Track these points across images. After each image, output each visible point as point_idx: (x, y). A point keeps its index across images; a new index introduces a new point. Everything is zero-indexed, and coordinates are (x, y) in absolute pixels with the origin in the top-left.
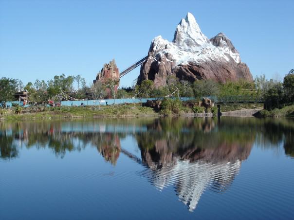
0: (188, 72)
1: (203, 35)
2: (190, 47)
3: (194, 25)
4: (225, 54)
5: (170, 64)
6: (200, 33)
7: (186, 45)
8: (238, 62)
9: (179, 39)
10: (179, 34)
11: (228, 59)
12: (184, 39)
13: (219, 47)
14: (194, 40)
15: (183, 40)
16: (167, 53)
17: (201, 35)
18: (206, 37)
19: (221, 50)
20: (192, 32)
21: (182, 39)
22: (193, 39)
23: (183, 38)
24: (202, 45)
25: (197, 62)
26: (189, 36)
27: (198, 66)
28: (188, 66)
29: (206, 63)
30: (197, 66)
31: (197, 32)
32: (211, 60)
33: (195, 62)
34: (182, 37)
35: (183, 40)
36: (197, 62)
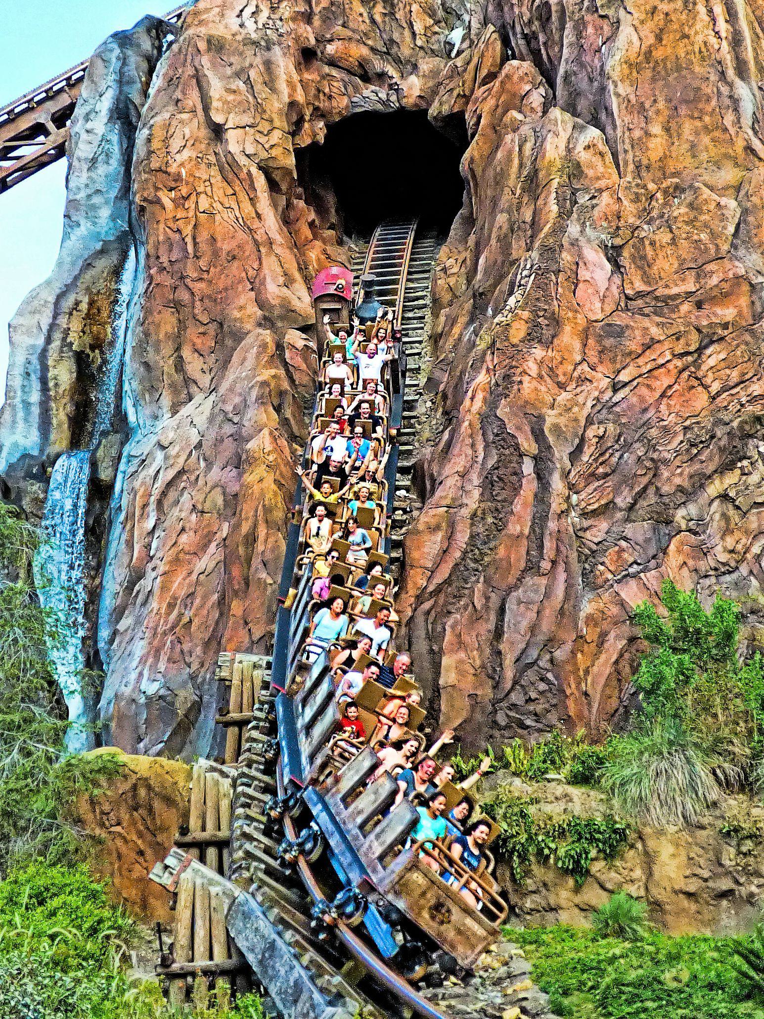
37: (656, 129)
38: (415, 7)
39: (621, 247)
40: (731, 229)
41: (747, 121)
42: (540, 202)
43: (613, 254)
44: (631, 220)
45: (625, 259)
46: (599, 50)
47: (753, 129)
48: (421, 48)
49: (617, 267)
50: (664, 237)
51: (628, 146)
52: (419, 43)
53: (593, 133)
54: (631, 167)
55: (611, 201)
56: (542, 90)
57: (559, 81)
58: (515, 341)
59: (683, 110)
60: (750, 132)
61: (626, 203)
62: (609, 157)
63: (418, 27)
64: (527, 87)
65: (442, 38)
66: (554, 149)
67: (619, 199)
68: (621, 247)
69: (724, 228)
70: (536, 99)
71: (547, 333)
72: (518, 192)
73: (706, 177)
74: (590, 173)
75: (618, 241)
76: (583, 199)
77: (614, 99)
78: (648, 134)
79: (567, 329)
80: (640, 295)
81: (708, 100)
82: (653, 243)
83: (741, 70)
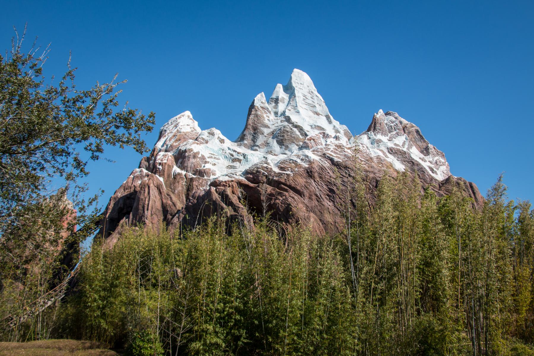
0: (403, 270)
1: (336, 123)
3: (309, 96)
4: (391, 151)
5: (183, 183)
6: (328, 117)
7: (274, 144)
8: (440, 177)
9: (255, 129)
10: (257, 116)
11: (400, 166)
12: (273, 128)
13: (371, 133)
14: (300, 129)
15: (266, 131)
17: (330, 122)
18: (345, 127)
19: (379, 141)
20: (298, 112)
22: (296, 127)
23: (267, 127)
25: (277, 170)
26: (288, 119)
27: (276, 184)
28: (240, 184)
29: (309, 173)
30: (270, 182)
31: (318, 114)
32: (332, 160)
33: (270, 170)
34: (266, 122)
35: (266, 131)
36: (277, 170)
83: (148, 210)
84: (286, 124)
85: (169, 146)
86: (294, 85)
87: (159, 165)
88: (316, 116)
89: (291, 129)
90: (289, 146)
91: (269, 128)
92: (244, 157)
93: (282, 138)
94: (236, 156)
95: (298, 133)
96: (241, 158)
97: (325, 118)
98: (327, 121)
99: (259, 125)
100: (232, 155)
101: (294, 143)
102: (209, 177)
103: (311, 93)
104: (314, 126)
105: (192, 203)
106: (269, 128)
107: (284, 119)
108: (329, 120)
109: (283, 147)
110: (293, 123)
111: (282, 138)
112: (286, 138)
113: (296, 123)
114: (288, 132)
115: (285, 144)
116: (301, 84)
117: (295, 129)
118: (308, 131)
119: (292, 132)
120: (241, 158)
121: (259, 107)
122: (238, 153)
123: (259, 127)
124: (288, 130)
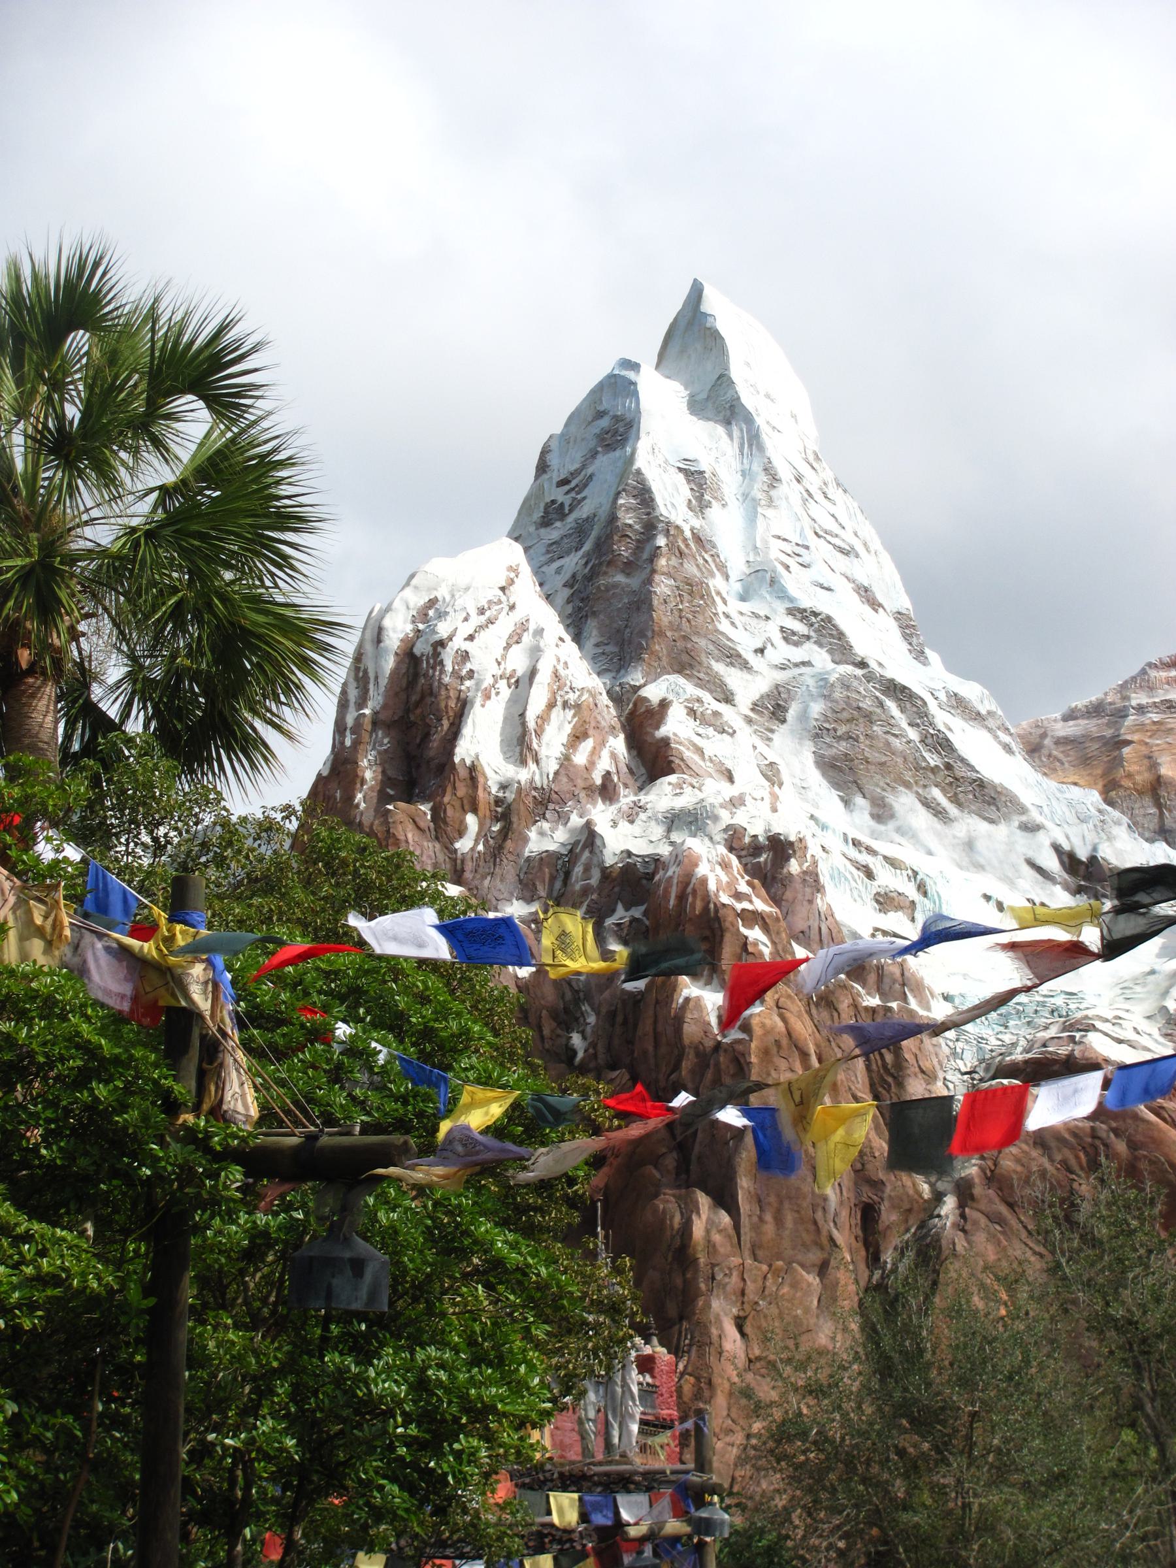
2: (882, 813)
3: (813, 481)
6: (907, 626)
16: (780, 848)
17: (919, 655)
21: (733, 677)
23: (733, 658)
24: (1027, 797)
34: (724, 626)
37: (768, 1217)
38: (544, 1012)
39: (745, 1318)
40: (815, 1302)
41: (831, 1216)
42: (689, 1276)
43: (740, 1323)
44: (751, 1297)
45: (748, 1329)
46: (727, 1143)
47: (834, 1221)
48: (548, 1051)
49: (743, 1334)
50: (774, 1310)
51: (747, 1229)
52: (547, 1046)
53: (725, 1218)
54: (748, 1245)
55: (739, 1280)
56: (675, 1155)
57: (694, 1158)
58: (685, 1399)
59: (786, 1205)
60: (832, 1224)
61: (748, 1283)
62: (735, 1240)
63: (546, 1032)
64: (664, 1150)
65: (564, 1041)
66: (698, 1229)
67: (744, 1280)
68: (745, 1318)
69: (812, 1302)
70: (670, 1161)
71: (707, 1394)
72: (670, 1259)
73: (799, 1257)
74: (722, 1250)
75: (742, 1314)
76: (719, 1277)
77: (740, 1192)
78: (761, 1219)
79: (719, 1392)
80: (758, 1359)
81: (805, 1198)
82: (765, 1317)
84: (821, 658)
85: (552, 767)
86: (748, 400)
87: (749, 925)
88: (867, 608)
89: (881, 705)
90: (890, 799)
91: (745, 666)
92: (922, 889)
93: (843, 746)
94: (887, 879)
95: (913, 734)
96: (911, 891)
97: (893, 626)
98: (905, 646)
99: (702, 643)
100: (870, 875)
101: (907, 785)
102: (928, 1009)
103: (811, 458)
104: (942, 696)
105: (1018, 1160)
106: (745, 666)
107: (799, 627)
108: (914, 641)
109: (859, 800)
110: (862, 664)
111: (843, 746)
112: (868, 753)
113: (880, 664)
114: (869, 717)
115: (869, 787)
116: (768, 396)
117: (891, 705)
118: (950, 729)
119: (889, 722)
120: (911, 891)
121: (688, 534)
122: (892, 862)
123: (703, 658)
124: (867, 704)
